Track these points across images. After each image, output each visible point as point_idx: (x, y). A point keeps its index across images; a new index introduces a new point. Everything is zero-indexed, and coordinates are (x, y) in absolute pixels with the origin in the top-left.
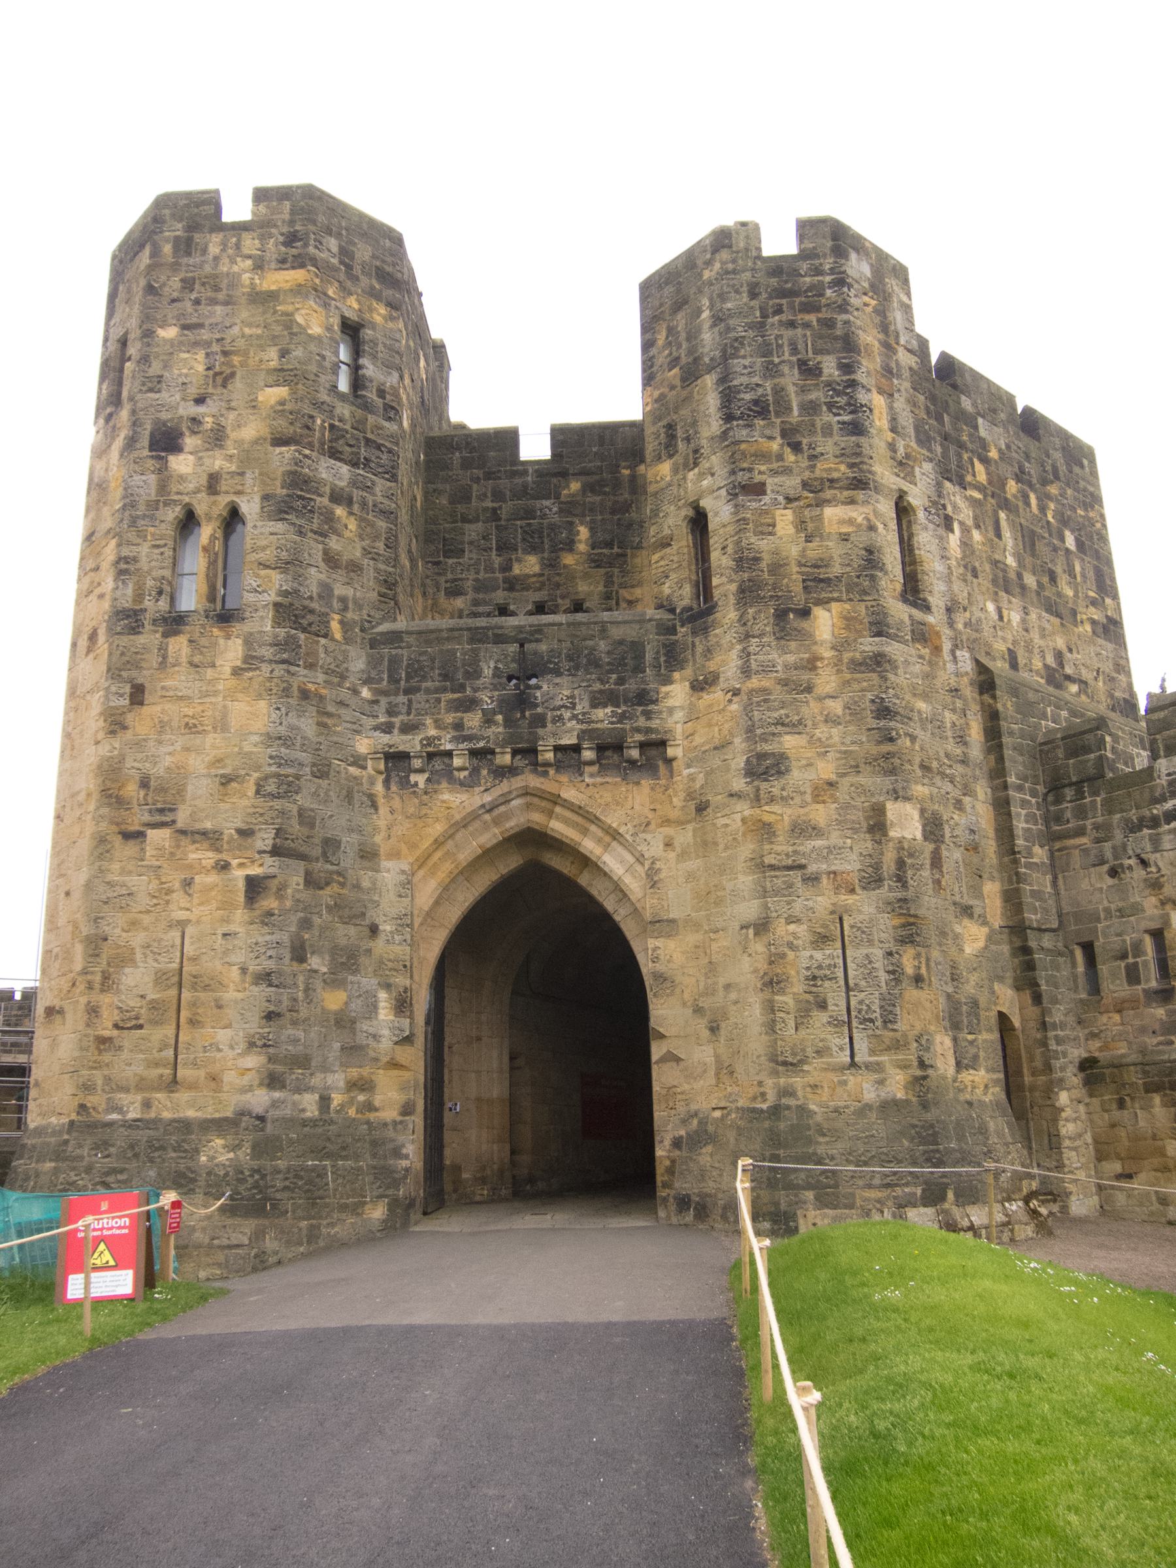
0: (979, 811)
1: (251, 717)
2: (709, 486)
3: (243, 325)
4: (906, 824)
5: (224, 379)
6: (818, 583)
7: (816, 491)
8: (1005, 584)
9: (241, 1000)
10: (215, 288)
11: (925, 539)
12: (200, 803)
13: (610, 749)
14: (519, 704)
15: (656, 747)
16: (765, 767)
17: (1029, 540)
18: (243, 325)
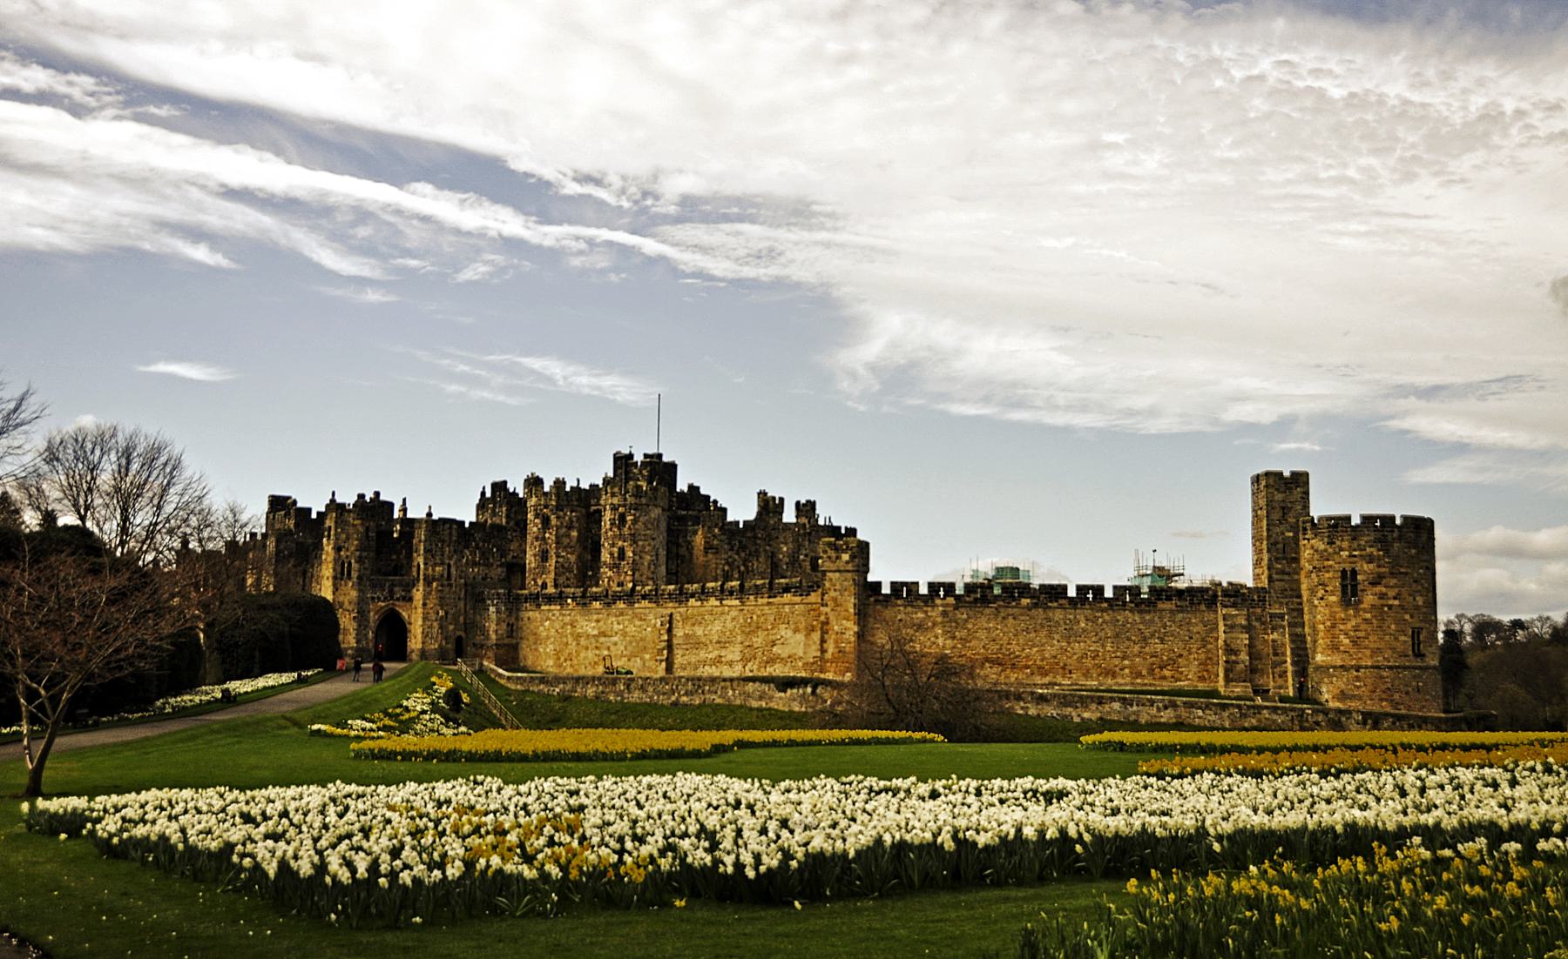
0: (461, 604)
1: (354, 594)
2: (421, 560)
3: (351, 530)
4: (441, 613)
5: (348, 539)
6: (434, 579)
7: (436, 564)
8: (475, 564)
9: (354, 634)
10: (346, 523)
11: (453, 571)
12: (346, 605)
13: (404, 599)
14: (391, 593)
15: (411, 599)
16: (424, 605)
17: (483, 554)
18: (351, 530)
